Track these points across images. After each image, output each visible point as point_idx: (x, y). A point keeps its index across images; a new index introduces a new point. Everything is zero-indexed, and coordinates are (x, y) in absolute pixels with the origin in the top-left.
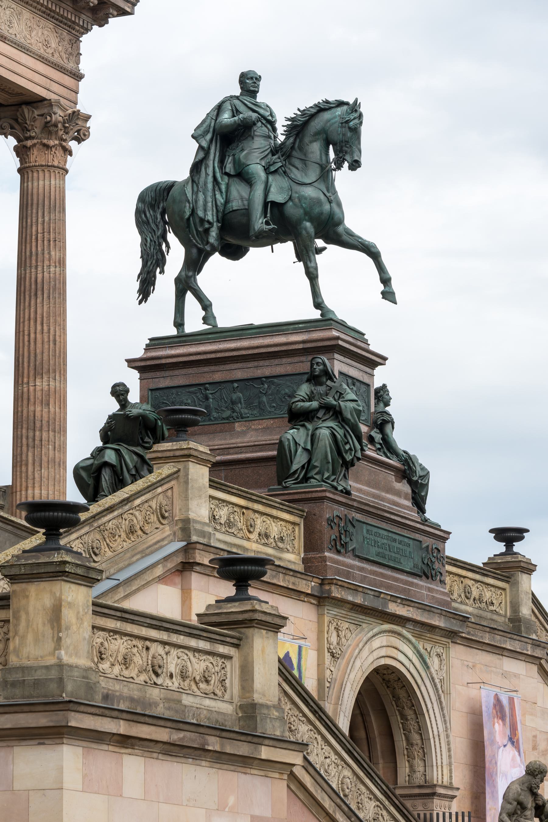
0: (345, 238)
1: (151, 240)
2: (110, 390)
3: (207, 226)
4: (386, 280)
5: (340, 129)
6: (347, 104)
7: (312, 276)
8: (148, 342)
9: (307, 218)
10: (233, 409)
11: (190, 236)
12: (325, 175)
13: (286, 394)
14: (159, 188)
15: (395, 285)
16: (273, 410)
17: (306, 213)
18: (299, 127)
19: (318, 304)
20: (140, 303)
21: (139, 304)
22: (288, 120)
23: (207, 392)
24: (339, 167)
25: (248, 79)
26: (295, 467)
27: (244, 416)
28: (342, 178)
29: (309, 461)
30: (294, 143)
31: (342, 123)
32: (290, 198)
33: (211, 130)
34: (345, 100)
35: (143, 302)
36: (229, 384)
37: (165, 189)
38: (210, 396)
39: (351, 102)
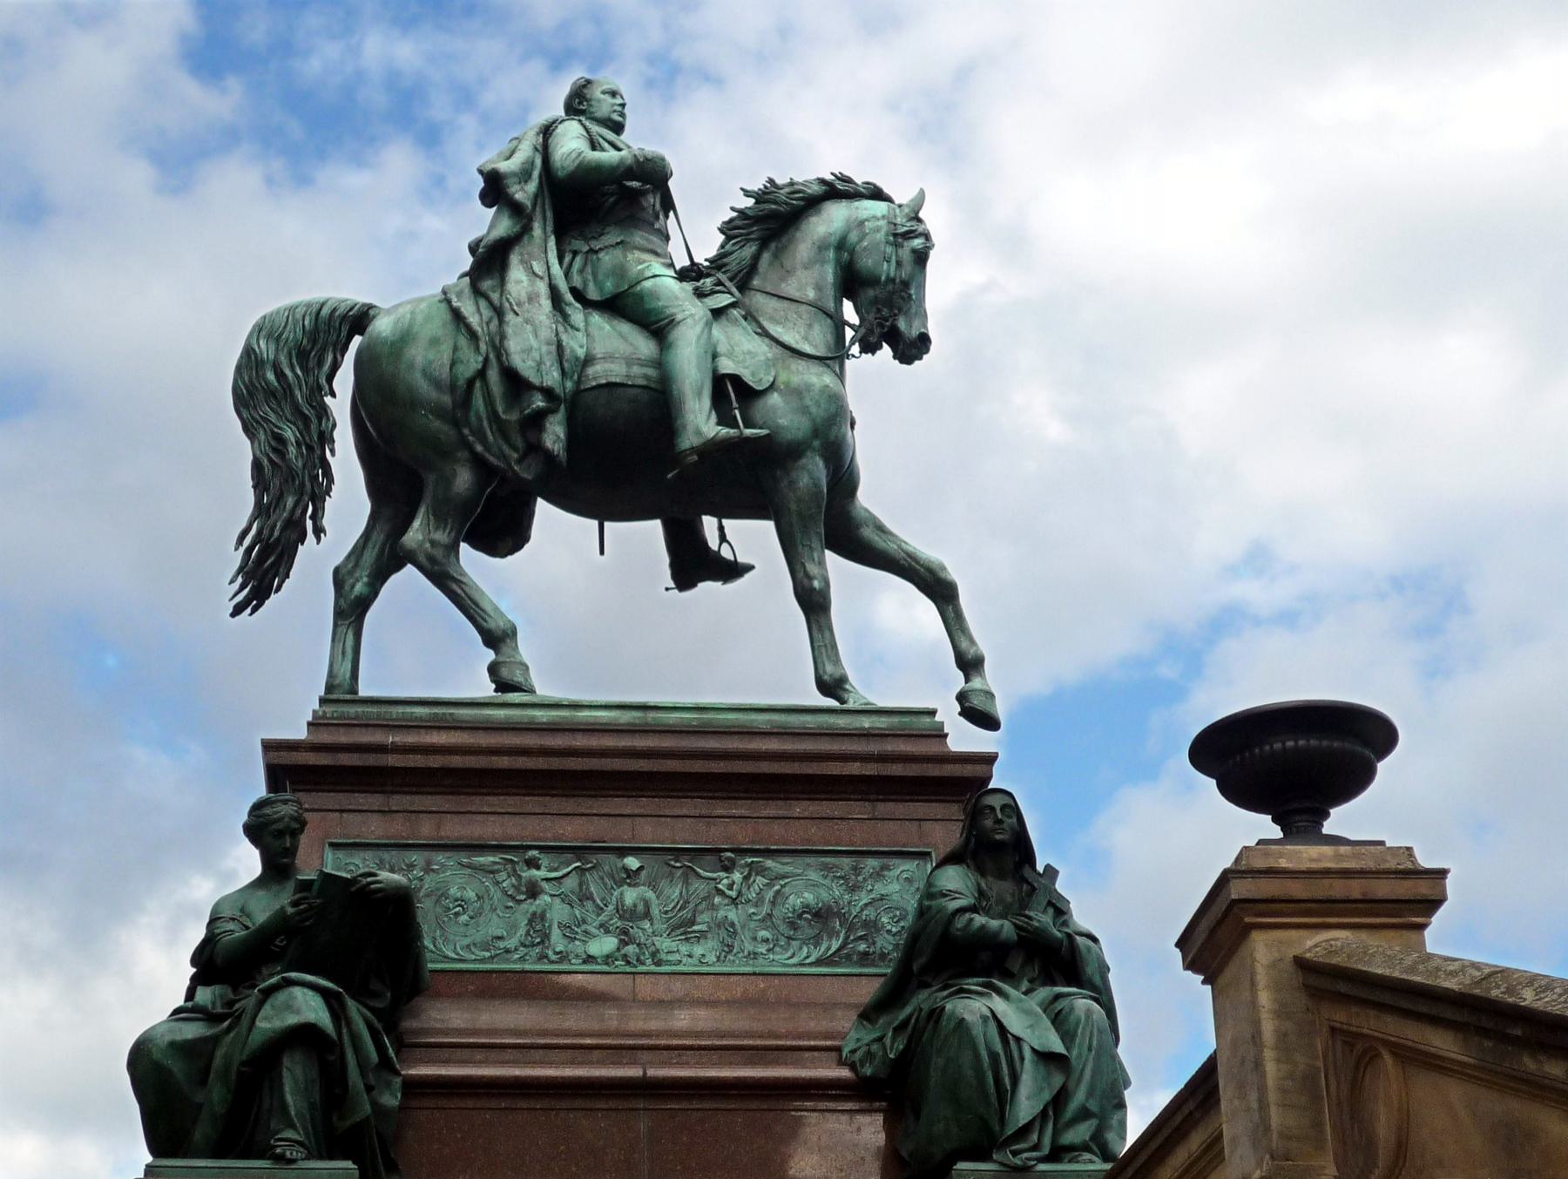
0: (868, 533)
1: (298, 444)
2: (245, 818)
3: (539, 402)
4: (969, 664)
5: (889, 249)
6: (888, 199)
7: (814, 603)
8: (317, 707)
9: (816, 443)
10: (625, 932)
11: (466, 431)
12: (835, 358)
13: (807, 906)
14: (325, 311)
15: (992, 677)
16: (762, 949)
17: (816, 433)
18: (772, 219)
19: (832, 686)
20: (237, 611)
21: (233, 615)
22: (747, 193)
23: (534, 872)
24: (869, 347)
25: (604, 93)
26: (1026, 1106)
27: (663, 956)
28: (871, 377)
29: (1059, 1100)
30: (756, 258)
31: (895, 235)
32: (772, 387)
33: (536, 174)
34: (887, 190)
35: (249, 610)
36: (612, 858)
37: (344, 317)
38: (545, 885)
39: (902, 195)
